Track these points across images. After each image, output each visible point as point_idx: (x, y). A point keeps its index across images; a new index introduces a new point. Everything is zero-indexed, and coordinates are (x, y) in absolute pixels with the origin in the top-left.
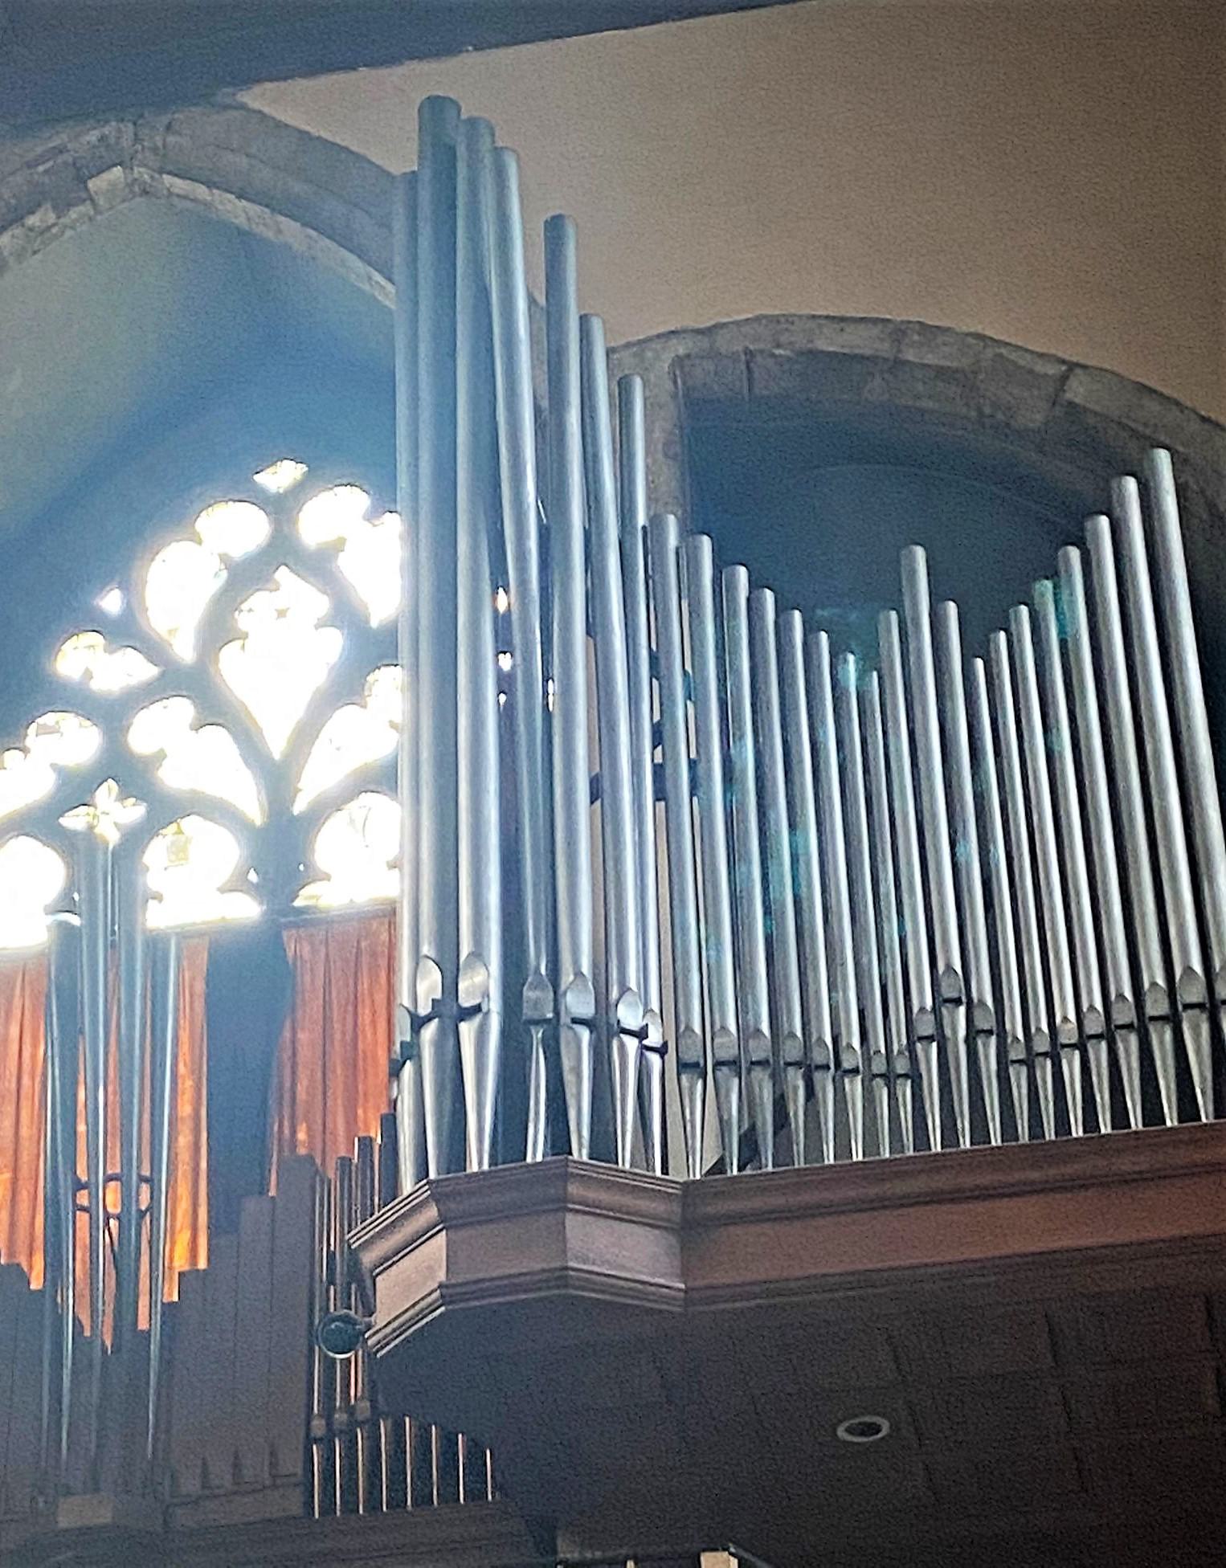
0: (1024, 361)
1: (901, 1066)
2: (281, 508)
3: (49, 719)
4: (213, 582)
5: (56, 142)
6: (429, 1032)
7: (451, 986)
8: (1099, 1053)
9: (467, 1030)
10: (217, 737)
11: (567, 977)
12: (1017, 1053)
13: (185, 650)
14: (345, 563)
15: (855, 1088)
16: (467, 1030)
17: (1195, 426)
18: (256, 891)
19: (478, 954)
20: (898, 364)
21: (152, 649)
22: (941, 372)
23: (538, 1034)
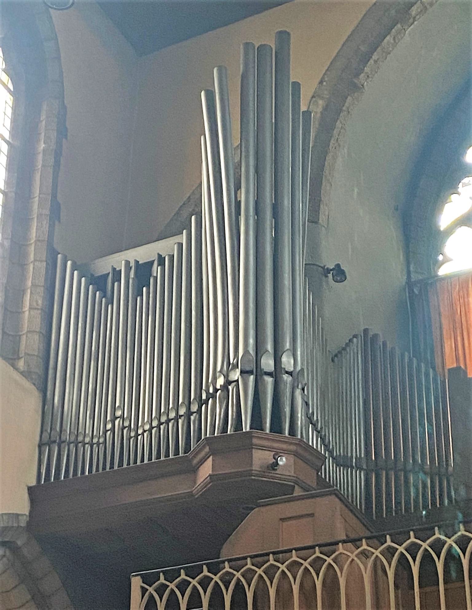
3: (466, 180)
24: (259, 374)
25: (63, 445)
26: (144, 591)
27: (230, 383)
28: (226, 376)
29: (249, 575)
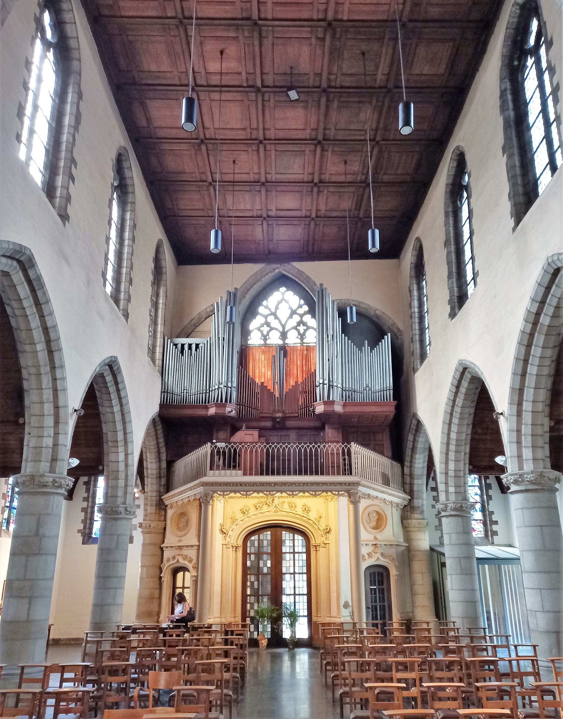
2: (283, 294)
4: (277, 303)
6: (321, 385)
9: (325, 386)
13: (273, 310)
16: (325, 386)
20: (360, 306)
21: (270, 310)
29: (238, 446)
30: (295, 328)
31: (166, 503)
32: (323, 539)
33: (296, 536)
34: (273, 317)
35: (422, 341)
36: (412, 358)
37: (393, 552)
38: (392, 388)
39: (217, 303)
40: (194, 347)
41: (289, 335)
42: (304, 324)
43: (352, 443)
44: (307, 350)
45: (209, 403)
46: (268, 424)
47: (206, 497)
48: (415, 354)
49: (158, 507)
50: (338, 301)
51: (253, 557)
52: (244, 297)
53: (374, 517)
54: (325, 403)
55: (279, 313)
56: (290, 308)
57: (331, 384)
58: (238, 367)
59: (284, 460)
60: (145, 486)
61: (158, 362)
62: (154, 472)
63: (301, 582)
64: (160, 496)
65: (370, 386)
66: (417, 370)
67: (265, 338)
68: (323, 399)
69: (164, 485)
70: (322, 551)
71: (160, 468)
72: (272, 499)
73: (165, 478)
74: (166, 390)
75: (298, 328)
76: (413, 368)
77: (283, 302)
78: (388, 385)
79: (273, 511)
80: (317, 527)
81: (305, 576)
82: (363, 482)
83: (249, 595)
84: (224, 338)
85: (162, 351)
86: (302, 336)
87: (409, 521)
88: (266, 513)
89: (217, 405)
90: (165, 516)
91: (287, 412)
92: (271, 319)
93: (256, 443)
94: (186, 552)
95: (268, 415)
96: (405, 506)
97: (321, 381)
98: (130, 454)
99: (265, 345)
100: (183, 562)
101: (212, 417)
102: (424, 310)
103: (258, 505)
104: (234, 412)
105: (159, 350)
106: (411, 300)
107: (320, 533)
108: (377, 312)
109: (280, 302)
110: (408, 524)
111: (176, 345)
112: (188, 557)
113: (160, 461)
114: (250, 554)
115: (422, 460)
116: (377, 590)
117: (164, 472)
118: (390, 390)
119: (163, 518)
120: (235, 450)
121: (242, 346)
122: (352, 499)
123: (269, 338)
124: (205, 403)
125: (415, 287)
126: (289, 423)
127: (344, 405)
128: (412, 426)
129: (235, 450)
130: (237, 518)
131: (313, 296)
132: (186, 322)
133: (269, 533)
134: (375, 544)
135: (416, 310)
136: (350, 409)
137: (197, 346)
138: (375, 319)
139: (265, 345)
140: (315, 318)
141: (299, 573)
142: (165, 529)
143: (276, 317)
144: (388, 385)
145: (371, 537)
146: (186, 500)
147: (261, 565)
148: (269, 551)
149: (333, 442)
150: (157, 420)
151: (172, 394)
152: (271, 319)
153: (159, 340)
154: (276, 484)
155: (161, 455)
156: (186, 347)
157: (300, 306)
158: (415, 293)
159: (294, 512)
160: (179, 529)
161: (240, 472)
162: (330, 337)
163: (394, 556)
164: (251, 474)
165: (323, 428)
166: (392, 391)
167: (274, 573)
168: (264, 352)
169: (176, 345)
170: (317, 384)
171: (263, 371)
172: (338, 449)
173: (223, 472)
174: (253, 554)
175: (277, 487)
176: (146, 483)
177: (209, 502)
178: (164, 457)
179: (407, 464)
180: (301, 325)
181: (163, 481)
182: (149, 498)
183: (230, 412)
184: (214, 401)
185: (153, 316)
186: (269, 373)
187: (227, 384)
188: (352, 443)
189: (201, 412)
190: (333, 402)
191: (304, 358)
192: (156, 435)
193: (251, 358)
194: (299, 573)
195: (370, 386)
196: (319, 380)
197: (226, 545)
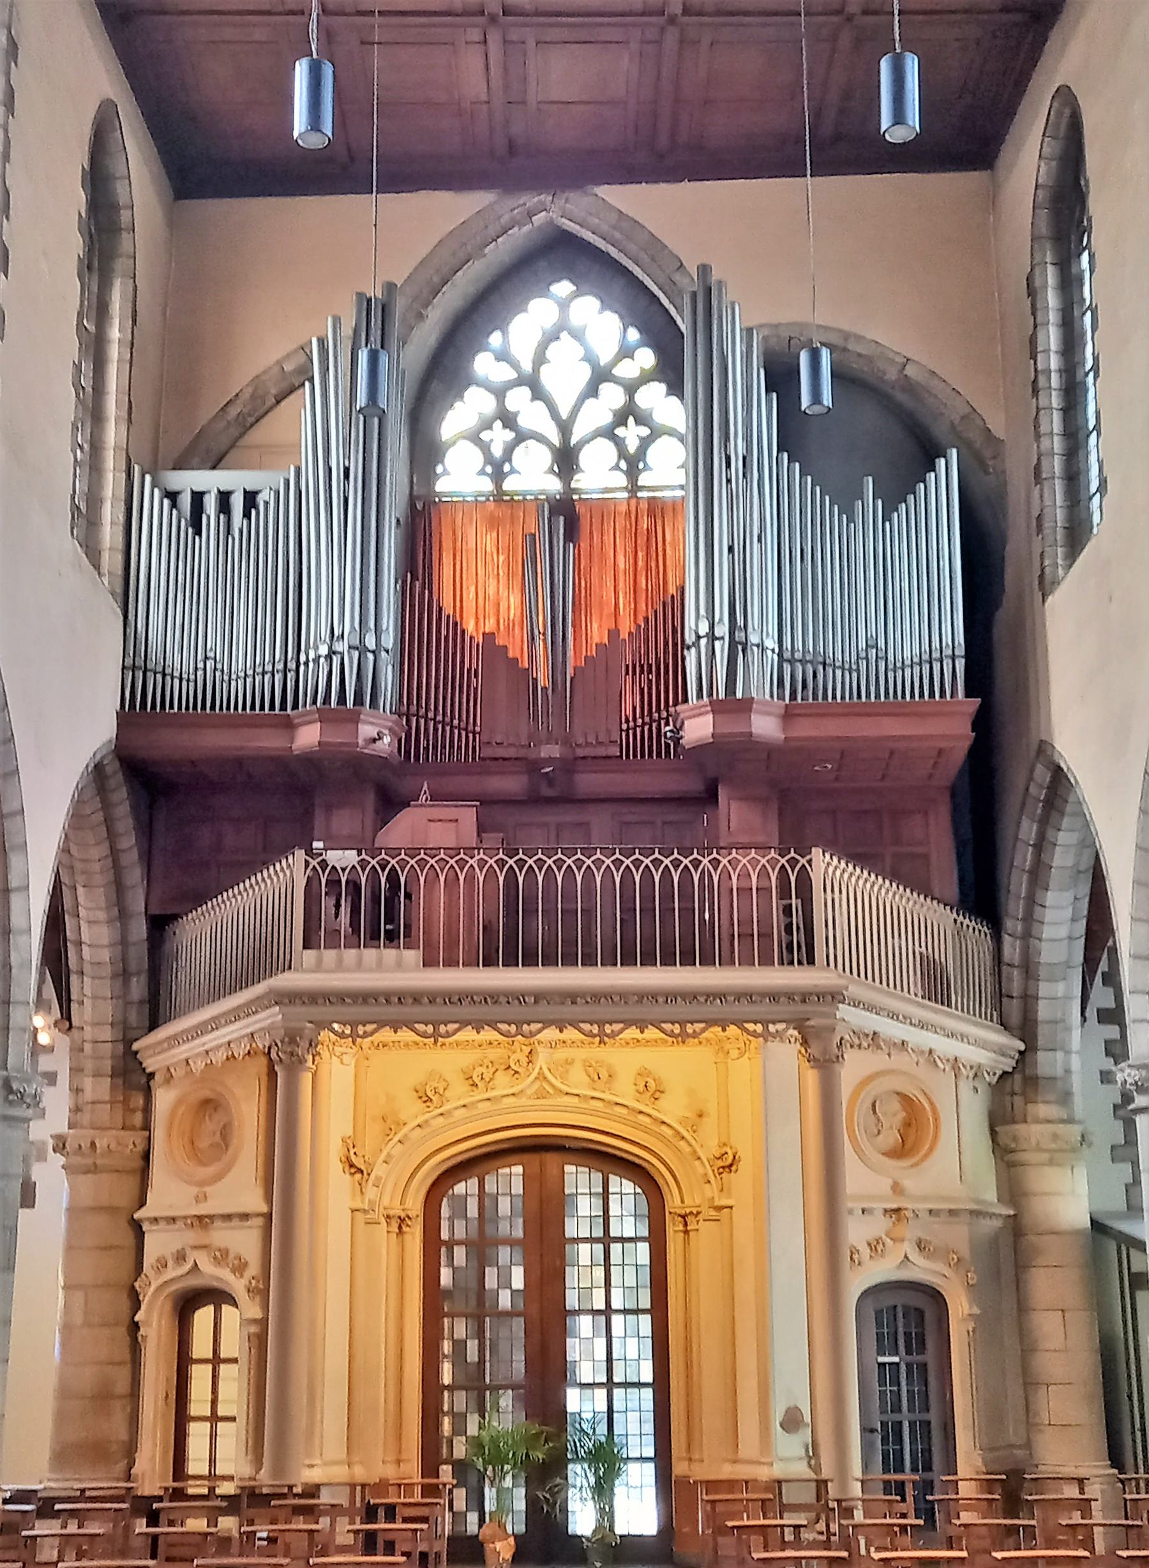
0: (891, 355)
1: (854, 667)
2: (564, 305)
4: (538, 337)
5: (521, 202)
7: (712, 627)
8: (917, 669)
9: (717, 644)
10: (539, 404)
11: (750, 629)
12: (891, 666)
13: (527, 367)
14: (589, 336)
15: (839, 673)
17: (949, 391)
18: (559, 475)
19: (721, 620)
20: (845, 350)
21: (515, 365)
22: (860, 355)
23: (740, 647)
24: (362, 649)
25: (148, 674)
26: (307, 863)
27: (334, 653)
28: (330, 648)
30: (608, 433)
31: (150, 1064)
32: (711, 1191)
33: (614, 1180)
34: (525, 392)
35: (1074, 477)
36: (1037, 541)
37: (959, 1237)
38: (961, 651)
39: (322, 342)
40: (237, 503)
41: (585, 458)
42: (642, 419)
43: (817, 852)
44: (651, 513)
45: (295, 706)
46: (511, 784)
47: (293, 1041)
48: (1047, 525)
49: (120, 1081)
50: (766, 332)
51: (460, 1253)
52: (420, 317)
53: (893, 1116)
54: (717, 708)
55: (547, 377)
56: (589, 358)
57: (740, 636)
58: (401, 578)
59: (569, 913)
60: (74, 1006)
61: (111, 560)
62: (105, 955)
63: (632, 1343)
64: (128, 1042)
65: (881, 643)
66: (1056, 583)
67: (498, 470)
68: (710, 694)
69: (141, 1002)
70: (705, 1233)
71: (123, 942)
72: (527, 1050)
73: (144, 978)
74: (140, 662)
75: (620, 431)
76: (1042, 576)
77: (564, 335)
78: (947, 639)
79: (529, 1092)
80: (688, 1149)
81: (646, 1321)
82: (854, 990)
83: (448, 1388)
84: (347, 470)
85: (121, 518)
86: (633, 463)
87: (1020, 1128)
88: (506, 1101)
89: (325, 717)
90: (147, 1110)
91: (581, 741)
92: (518, 400)
93: (470, 854)
94: (221, 1236)
95: (511, 753)
96: (1005, 1073)
97: (704, 628)
98: (18, 889)
99: (499, 495)
100: (212, 1273)
101: (309, 760)
102: (1083, 363)
103: (479, 1070)
104: (387, 740)
105: (110, 514)
106: (1035, 327)
107: (701, 1170)
108: (910, 371)
109: (551, 337)
110: (1015, 1139)
111: (173, 496)
112: (231, 1256)
113: (123, 915)
114: (450, 1245)
115: (1068, 913)
116: (903, 1368)
117: (139, 954)
118: (953, 658)
119: (138, 1119)
120: (393, 878)
121: (412, 499)
122: (814, 1050)
123: (513, 471)
124: (283, 707)
125: (1051, 276)
126: (588, 782)
127: (788, 716)
128: (1033, 790)
129: (393, 878)
130: (403, 1117)
131: (673, 311)
132: (207, 412)
133: (518, 1169)
134: (898, 1210)
135: (1054, 362)
136: (806, 729)
137: (250, 498)
138: (900, 397)
139: (499, 495)
140: (681, 396)
141: (625, 1312)
142: (146, 1156)
143: (538, 393)
144: (947, 639)
145: (883, 1185)
146: (221, 1055)
147: (491, 1281)
148: (519, 1233)
149: (746, 847)
150: (113, 767)
151: (164, 675)
152: (518, 400)
153: (110, 476)
154: (540, 996)
155: (129, 895)
156: (211, 504)
157: (626, 352)
158: (1052, 299)
159: (606, 1096)
160: (197, 1156)
161: (413, 956)
162: (737, 464)
163: (965, 1252)
164: (451, 963)
165: (710, 797)
166: (960, 664)
167: (534, 1309)
168: (493, 523)
169: (173, 496)
170: (690, 638)
171: (491, 591)
172: (764, 874)
173: (351, 954)
174: (459, 1243)
175: (543, 1010)
176: (74, 996)
177: (302, 1061)
178: (137, 902)
179: (1013, 925)
180: (631, 420)
181: (138, 988)
182: (88, 1047)
183: (374, 740)
184: (314, 702)
185: (89, 390)
186: (515, 600)
187: (362, 640)
188: (817, 852)
189: (268, 741)
190: (746, 706)
191: (642, 541)
192: (109, 822)
193: (447, 544)
194: (625, 1312)
195: (881, 643)
196: (695, 623)
197: (365, 1211)
